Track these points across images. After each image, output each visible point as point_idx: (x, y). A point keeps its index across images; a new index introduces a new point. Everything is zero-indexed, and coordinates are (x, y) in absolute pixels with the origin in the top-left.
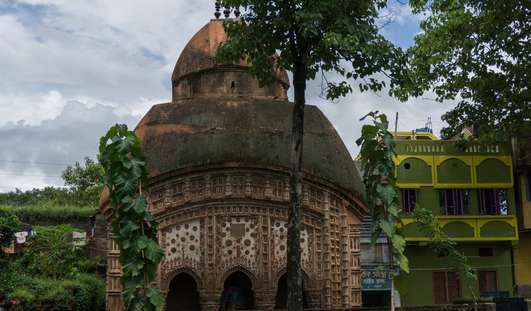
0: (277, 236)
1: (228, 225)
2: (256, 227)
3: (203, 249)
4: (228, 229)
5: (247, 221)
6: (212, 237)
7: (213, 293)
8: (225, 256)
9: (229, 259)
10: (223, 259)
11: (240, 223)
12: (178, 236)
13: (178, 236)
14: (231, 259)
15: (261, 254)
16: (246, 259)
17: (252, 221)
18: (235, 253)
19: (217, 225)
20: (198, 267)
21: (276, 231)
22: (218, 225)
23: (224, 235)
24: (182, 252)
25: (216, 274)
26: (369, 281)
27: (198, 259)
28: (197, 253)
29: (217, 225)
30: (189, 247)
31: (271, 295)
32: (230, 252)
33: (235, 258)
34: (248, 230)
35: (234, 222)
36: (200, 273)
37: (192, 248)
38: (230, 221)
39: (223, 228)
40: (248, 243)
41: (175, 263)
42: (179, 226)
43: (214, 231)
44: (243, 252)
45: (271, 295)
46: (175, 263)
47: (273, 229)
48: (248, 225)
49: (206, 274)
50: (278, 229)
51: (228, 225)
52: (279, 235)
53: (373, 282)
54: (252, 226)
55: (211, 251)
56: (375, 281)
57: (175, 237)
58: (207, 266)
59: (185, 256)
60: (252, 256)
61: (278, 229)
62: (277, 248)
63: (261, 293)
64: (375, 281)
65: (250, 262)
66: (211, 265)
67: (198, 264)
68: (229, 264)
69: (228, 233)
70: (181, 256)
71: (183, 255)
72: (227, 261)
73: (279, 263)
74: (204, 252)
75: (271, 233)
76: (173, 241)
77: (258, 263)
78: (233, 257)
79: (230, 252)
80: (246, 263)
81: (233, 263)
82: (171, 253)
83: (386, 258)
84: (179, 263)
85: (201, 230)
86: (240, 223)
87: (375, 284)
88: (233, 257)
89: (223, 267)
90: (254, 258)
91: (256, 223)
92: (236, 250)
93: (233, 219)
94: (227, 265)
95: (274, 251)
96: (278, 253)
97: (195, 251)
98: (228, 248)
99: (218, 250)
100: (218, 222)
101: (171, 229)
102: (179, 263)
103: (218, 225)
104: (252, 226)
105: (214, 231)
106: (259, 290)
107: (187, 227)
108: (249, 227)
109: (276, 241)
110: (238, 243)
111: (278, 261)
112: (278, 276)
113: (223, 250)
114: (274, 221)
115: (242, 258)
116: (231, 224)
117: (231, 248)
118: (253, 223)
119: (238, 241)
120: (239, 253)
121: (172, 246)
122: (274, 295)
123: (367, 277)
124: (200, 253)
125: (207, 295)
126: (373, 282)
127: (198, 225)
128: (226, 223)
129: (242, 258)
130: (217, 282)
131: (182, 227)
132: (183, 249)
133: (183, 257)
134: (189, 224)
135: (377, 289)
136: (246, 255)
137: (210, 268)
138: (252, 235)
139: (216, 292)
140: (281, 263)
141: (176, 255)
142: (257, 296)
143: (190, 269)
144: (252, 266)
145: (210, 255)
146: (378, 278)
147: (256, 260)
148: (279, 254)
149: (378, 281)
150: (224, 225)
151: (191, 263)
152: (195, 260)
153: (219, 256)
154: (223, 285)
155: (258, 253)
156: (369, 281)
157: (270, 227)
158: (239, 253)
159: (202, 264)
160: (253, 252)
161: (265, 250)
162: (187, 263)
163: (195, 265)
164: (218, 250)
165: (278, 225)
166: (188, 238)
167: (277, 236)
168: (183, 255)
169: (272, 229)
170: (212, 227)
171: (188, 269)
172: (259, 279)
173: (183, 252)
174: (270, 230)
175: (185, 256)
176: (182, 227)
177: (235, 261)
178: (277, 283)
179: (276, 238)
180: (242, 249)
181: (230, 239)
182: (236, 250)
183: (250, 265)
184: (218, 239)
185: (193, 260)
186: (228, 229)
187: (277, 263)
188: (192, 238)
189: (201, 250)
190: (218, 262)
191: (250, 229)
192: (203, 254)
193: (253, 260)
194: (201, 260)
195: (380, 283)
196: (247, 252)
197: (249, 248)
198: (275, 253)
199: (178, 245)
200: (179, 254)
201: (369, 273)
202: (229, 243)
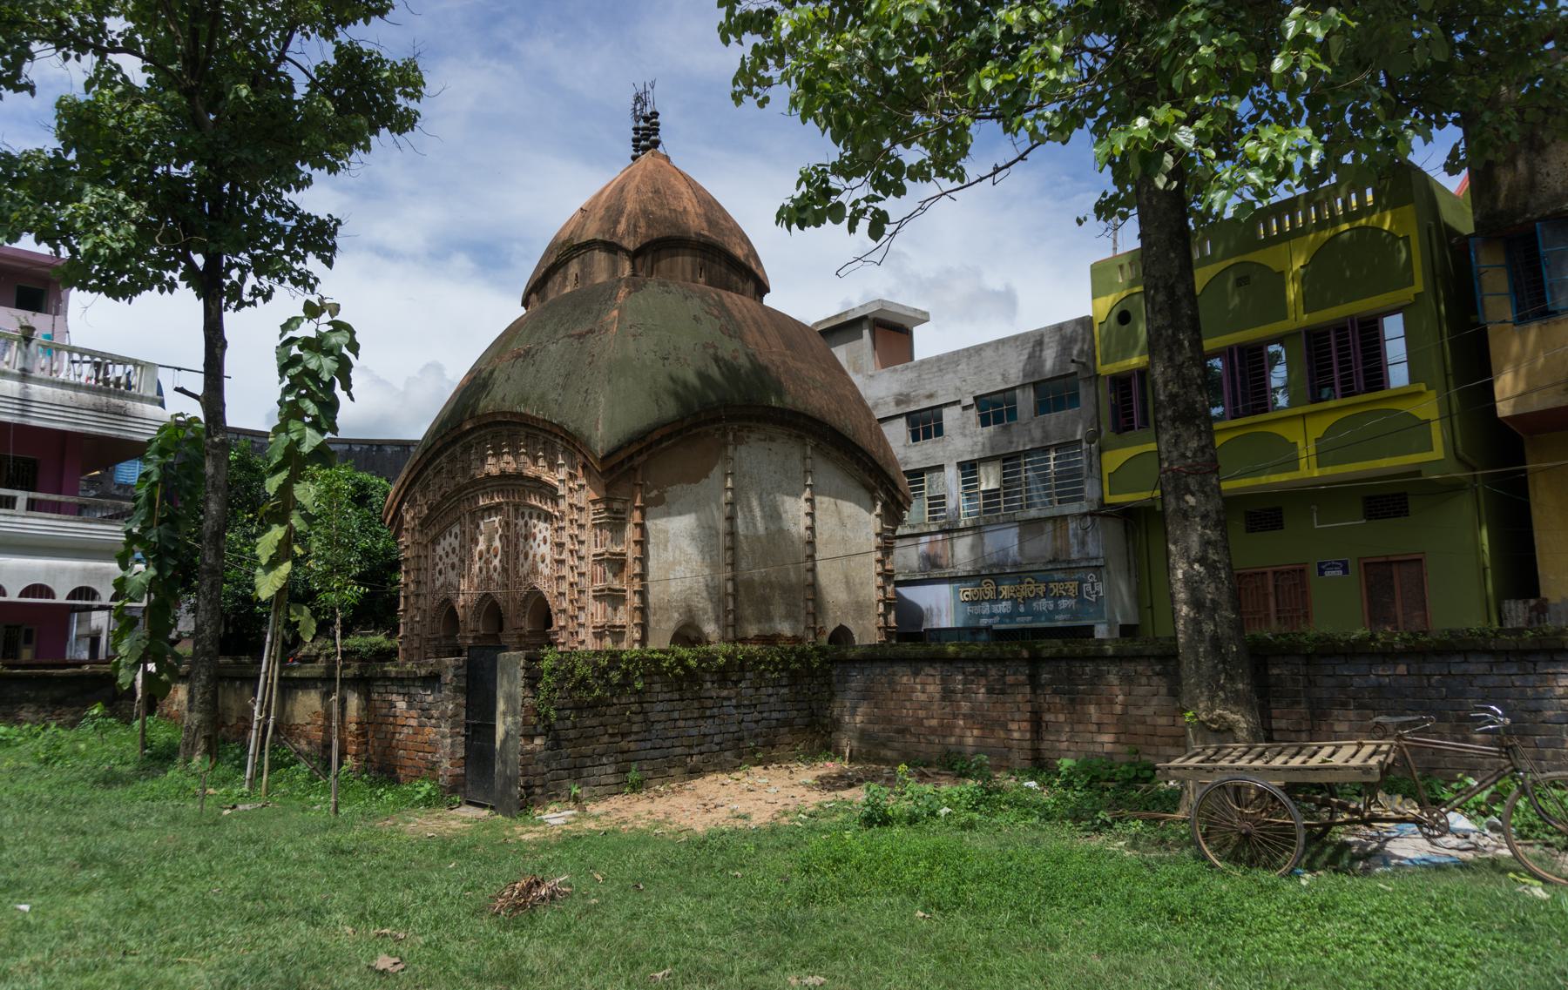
26: (1043, 605)
50: (521, 522)
53: (1051, 607)
56: (1056, 605)
61: (521, 522)
62: (522, 556)
64: (1056, 605)
83: (1076, 548)
87: (1056, 611)
123: (1037, 597)
126: (1051, 607)
135: (1059, 624)
146: (1061, 596)
149: (1063, 603)
156: (1043, 605)
195: (1068, 610)
201: (1042, 587)
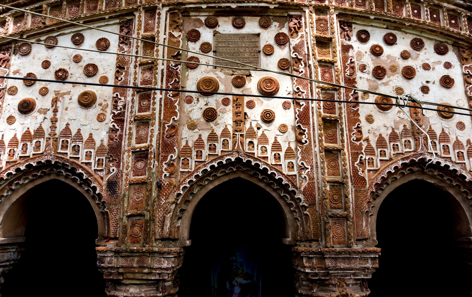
0: (363, 68)
1: (207, 35)
2: (294, 41)
3: (120, 104)
4: (205, 48)
5: (265, 26)
6: (150, 67)
7: (142, 254)
8: (192, 126)
9: (205, 136)
10: (187, 136)
11: (244, 31)
12: (46, 65)
13: (46, 65)
14: (213, 137)
15: (315, 120)
16: (264, 139)
17: (282, 26)
18: (226, 119)
19: (171, 35)
20: (99, 163)
21: (359, 54)
22: (176, 34)
23: (193, 64)
24: (50, 114)
25: (159, 186)
27: (102, 136)
28: (100, 118)
29: (171, 35)
30: (75, 98)
31: (357, 264)
32: (210, 115)
33: (225, 133)
34: (269, 52)
35: (226, 26)
36: (104, 183)
37: (87, 101)
38: (211, 25)
39: (191, 45)
40: (268, 91)
41: (25, 146)
42: (55, 39)
43: (161, 53)
44: (255, 115)
45: (357, 264)
46: (25, 146)
47: (351, 47)
48: (267, 37)
49: (123, 185)
51: (207, 35)
52: (371, 67)
54: (281, 40)
55: (148, 108)
57: (39, 72)
58: (127, 158)
59: (60, 126)
60: (283, 129)
63: (321, 256)
65: (277, 146)
66: (142, 155)
67: (100, 151)
68: (206, 152)
69: (207, 59)
70: (46, 126)
71: (54, 121)
72: (199, 143)
73: (377, 152)
74: (122, 114)
75: (345, 59)
76: (30, 80)
77: (307, 152)
78: (219, 132)
79: (210, 115)
80: (264, 150)
81: (219, 148)
82: (17, 114)
84: (38, 147)
85: (121, 49)
86: (244, 31)
88: (219, 132)
89: (186, 164)
90: (291, 135)
91: (295, 31)
92: (230, 107)
93: (221, 20)
94: (199, 155)
95: (356, 113)
96: (370, 119)
97: (94, 111)
98: (203, 101)
99: (169, 108)
100: (175, 25)
101: (29, 46)
102: (38, 147)
103: (176, 34)
104: (281, 40)
105: (161, 53)
106: (314, 247)
107: (78, 40)
108: (272, 42)
109: (363, 81)
110: (238, 87)
111: (373, 144)
112: (375, 196)
113: (187, 107)
114: (350, 26)
115: (251, 133)
116: (215, 33)
117: (213, 102)
118: (285, 30)
119: (239, 82)
120: (240, 118)
121: (25, 93)
122: (369, 265)
124: (109, 117)
125: (121, 262)
127: (112, 34)
128: (201, 30)
129: (251, 133)
130: (159, 215)
131: (65, 41)
132: (55, 101)
133: (53, 127)
134: (86, 34)
136: (264, 126)
137: (140, 165)
138: (284, 66)
139: (152, 253)
140: (383, 154)
141: (31, 122)
142: (308, 267)
143: (72, 170)
144: (284, 163)
145: (143, 122)
147: (299, 141)
148: (374, 125)
150: (194, 36)
151: (76, 149)
152: (91, 139)
153: (172, 127)
154: (184, 226)
155: (303, 118)
157: (338, 40)
158: (240, 118)
159: (114, 151)
160: (286, 117)
161: (330, 108)
162: (65, 146)
163: (88, 155)
164: (169, 108)
165: (363, 37)
166: (77, 73)
167: (363, 68)
168: (54, 121)
169: (346, 49)
170: (153, 38)
171: (64, 166)
172: (312, 204)
173: (55, 111)
174: (339, 48)
175: (60, 126)
176: (65, 41)
177: (225, 144)
178: (373, 220)
179: (359, 74)
180: (251, 105)
181: (211, 75)
182: (230, 107)
183: (277, 157)
184: (171, 74)
185: (85, 137)
186: (205, 48)
187: (370, 151)
188: (91, 70)
189: (115, 107)
190: (167, 146)
191: (276, 48)
192: (119, 119)
193: (288, 140)
194: (111, 138)
196: (268, 118)
197: (274, 105)
198: (362, 118)
199: (44, 92)
200: (41, 117)
202: (208, 88)
